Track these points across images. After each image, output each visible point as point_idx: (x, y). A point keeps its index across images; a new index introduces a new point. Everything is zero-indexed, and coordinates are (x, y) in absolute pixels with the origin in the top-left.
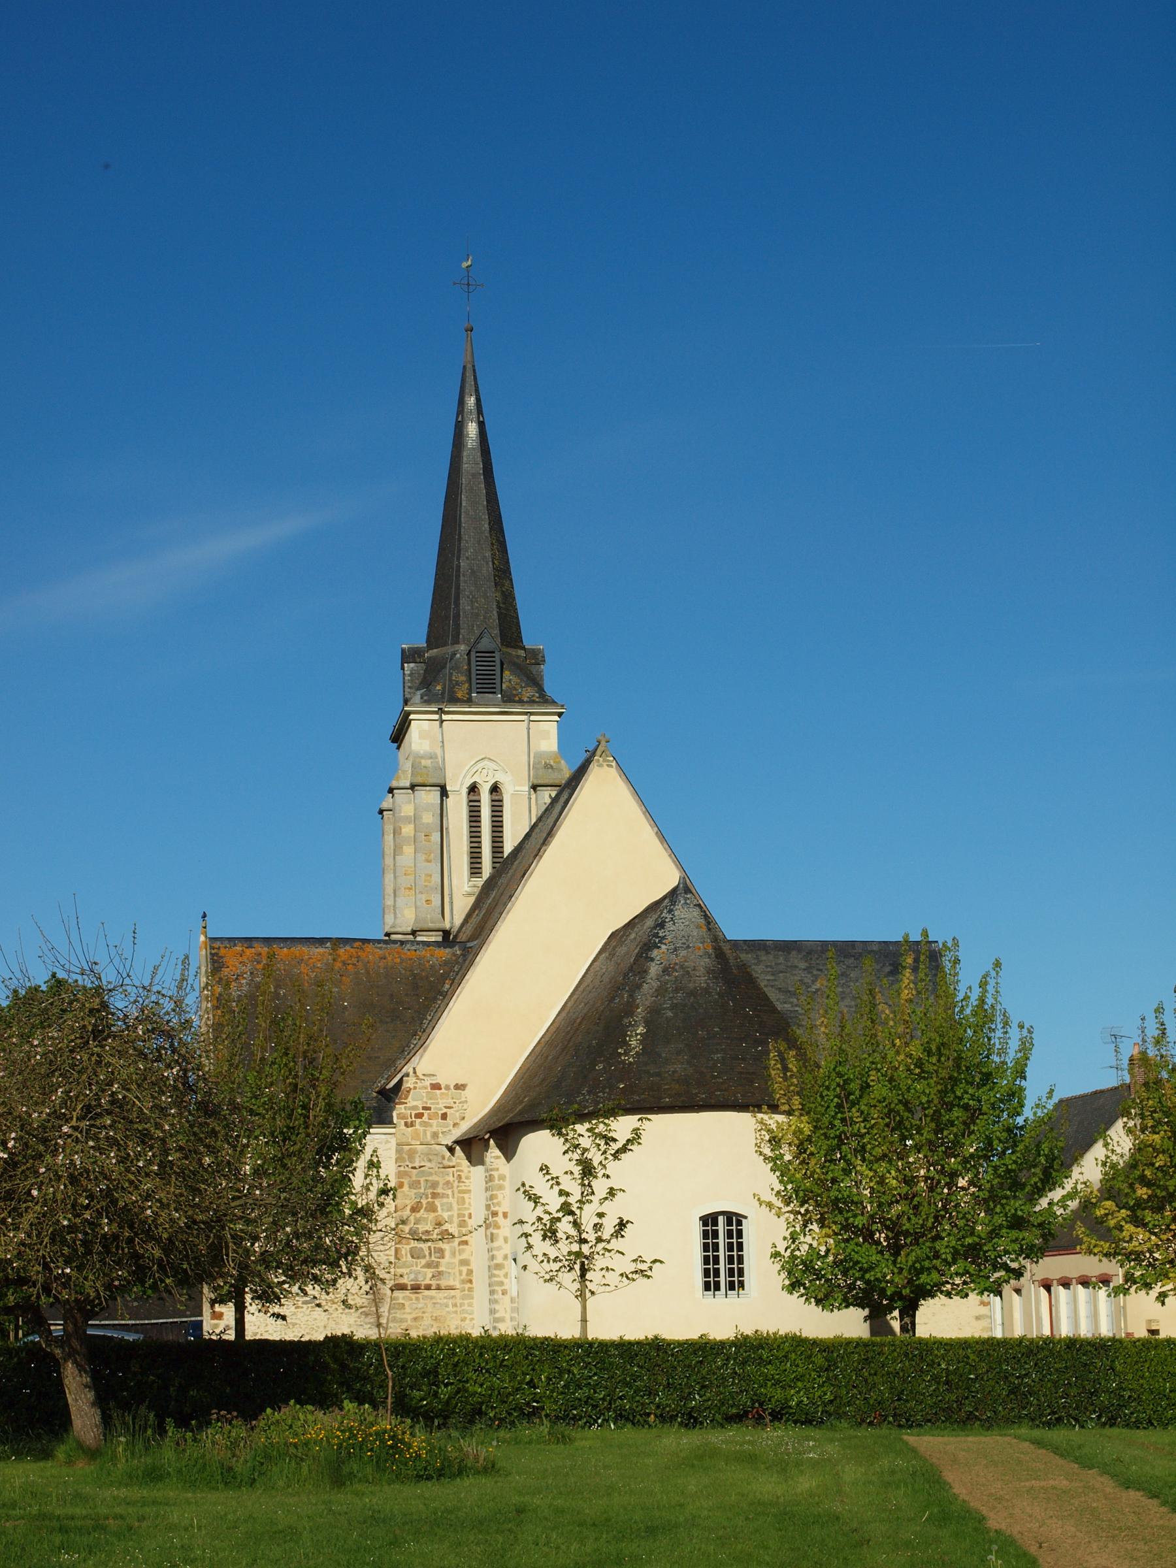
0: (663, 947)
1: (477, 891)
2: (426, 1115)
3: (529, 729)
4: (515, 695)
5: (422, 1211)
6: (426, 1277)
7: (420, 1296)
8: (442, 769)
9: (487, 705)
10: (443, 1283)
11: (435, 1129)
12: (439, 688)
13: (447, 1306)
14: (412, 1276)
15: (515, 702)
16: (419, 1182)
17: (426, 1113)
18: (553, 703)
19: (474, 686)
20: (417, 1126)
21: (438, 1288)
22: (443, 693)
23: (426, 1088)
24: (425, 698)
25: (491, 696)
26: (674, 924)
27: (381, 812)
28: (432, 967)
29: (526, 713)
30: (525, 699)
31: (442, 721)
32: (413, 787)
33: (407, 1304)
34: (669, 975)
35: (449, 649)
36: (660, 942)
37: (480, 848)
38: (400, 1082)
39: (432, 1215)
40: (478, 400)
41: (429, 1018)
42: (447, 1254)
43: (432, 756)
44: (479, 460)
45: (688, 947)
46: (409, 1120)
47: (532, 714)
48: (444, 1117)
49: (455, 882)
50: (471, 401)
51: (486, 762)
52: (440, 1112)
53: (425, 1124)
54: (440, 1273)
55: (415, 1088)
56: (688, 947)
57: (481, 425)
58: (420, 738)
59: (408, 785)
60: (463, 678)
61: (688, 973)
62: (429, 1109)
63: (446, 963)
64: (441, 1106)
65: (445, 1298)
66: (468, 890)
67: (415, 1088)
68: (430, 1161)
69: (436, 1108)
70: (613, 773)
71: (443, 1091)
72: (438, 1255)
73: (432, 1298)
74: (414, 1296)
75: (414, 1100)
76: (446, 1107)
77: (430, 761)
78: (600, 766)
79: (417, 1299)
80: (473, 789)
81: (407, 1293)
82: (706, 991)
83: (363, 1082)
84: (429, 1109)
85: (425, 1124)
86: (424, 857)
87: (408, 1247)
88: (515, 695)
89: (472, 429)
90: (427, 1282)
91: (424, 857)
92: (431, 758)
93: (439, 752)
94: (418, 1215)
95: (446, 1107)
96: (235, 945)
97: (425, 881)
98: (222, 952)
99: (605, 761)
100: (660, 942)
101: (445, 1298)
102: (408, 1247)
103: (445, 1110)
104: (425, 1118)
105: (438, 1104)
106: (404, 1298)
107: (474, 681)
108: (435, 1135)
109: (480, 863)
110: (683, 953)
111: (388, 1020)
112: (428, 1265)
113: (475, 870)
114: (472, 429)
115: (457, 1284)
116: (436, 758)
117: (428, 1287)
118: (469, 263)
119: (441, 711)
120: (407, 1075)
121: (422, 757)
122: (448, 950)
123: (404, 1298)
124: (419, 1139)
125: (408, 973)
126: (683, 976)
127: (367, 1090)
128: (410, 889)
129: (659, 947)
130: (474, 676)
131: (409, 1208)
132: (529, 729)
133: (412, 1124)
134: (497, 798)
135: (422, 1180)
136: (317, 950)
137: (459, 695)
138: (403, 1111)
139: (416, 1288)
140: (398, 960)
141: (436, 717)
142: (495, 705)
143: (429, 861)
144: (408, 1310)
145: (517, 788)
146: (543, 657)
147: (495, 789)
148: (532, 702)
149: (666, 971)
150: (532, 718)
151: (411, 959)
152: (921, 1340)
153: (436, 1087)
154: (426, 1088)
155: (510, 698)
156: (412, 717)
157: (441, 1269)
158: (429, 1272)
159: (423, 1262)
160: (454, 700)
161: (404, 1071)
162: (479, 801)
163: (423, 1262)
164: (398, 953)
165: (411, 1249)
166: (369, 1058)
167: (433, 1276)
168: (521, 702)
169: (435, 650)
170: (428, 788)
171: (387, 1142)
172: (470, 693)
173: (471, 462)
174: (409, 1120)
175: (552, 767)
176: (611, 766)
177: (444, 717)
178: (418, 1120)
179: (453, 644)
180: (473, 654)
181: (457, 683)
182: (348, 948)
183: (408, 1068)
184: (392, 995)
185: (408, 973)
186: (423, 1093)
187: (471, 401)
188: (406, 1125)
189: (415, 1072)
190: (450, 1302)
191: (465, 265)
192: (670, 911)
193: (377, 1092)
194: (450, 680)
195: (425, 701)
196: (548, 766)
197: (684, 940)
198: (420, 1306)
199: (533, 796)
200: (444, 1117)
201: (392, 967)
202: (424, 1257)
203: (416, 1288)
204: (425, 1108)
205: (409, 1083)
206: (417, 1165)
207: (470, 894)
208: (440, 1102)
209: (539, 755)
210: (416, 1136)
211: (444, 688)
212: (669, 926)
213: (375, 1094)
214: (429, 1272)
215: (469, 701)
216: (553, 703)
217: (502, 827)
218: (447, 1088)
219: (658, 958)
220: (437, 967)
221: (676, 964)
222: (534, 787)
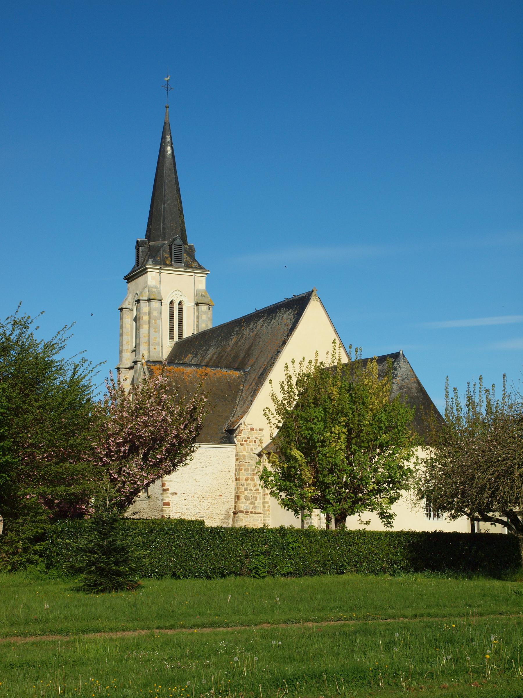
0: (398, 378)
1: (173, 346)
2: (248, 441)
3: (194, 279)
4: (189, 264)
5: (249, 481)
6: (250, 508)
7: (248, 516)
8: (160, 293)
9: (179, 268)
10: (257, 511)
11: (251, 447)
12: (158, 258)
13: (258, 520)
14: (245, 508)
15: (189, 267)
16: (248, 469)
17: (248, 440)
18: (204, 269)
19: (173, 259)
20: (245, 445)
21: (255, 513)
22: (161, 261)
23: (248, 430)
24: (154, 262)
25: (180, 264)
26: (401, 369)
27: (121, 309)
28: (234, 379)
29: (194, 273)
30: (193, 267)
31: (161, 273)
32: (149, 300)
33: (243, 519)
34: (403, 390)
35: (160, 243)
36: (395, 376)
37: (173, 328)
38: (239, 426)
39: (253, 482)
40: (171, 137)
41: (238, 400)
42: (258, 499)
43: (156, 287)
44: (172, 163)
45: (408, 379)
46: (242, 443)
47: (196, 273)
48: (255, 442)
49: (164, 341)
50: (169, 138)
51: (177, 292)
52: (254, 440)
53: (248, 445)
54: (255, 506)
55: (244, 429)
56: (408, 379)
57: (172, 148)
58: (151, 279)
59: (146, 299)
60: (168, 255)
61: (410, 389)
62: (249, 438)
63: (239, 378)
64: (254, 437)
65: (258, 517)
66: (169, 345)
67: (244, 429)
68: (252, 460)
69: (252, 438)
70: (318, 303)
71: (255, 431)
72: (255, 499)
73: (253, 517)
74: (246, 516)
75: (244, 434)
76: (256, 438)
77: (156, 289)
78: (314, 300)
79: (247, 517)
80: (171, 303)
81: (243, 514)
82: (417, 397)
83: (219, 426)
84: (249, 438)
85: (248, 445)
86: (153, 330)
87: (244, 495)
88: (189, 264)
89: (169, 149)
90: (251, 510)
91: (153, 330)
92: (156, 288)
93: (159, 286)
94: (248, 482)
95: (256, 438)
96: (156, 365)
97: (154, 340)
98: (152, 367)
99: (315, 299)
100: (395, 376)
101: (258, 517)
102: (244, 495)
103: (255, 439)
104: (248, 442)
105: (253, 436)
106: (242, 517)
107: (173, 257)
108: (252, 449)
109: (173, 334)
110: (407, 381)
111: (223, 400)
112: (251, 503)
113: (171, 337)
114: (169, 149)
115: (262, 511)
116: (158, 288)
117: (251, 512)
118: (169, 78)
119: (161, 269)
120: (241, 424)
121: (153, 288)
122: (238, 372)
123: (242, 517)
124: (245, 451)
125: (226, 381)
126: (408, 390)
127: (221, 429)
128: (146, 343)
129: (396, 378)
130: (173, 255)
131: (244, 479)
132: (194, 279)
133: (243, 445)
134: (180, 307)
135: (249, 468)
136: (189, 369)
137: (167, 262)
138: (240, 439)
139: (247, 512)
140: (221, 375)
141: (158, 271)
142: (182, 268)
143: (155, 332)
144: (244, 522)
145: (190, 304)
146: (194, 249)
147: (180, 303)
148: (196, 268)
149: (401, 388)
150: (196, 275)
151: (225, 375)
152: (350, 533)
153: (252, 429)
154: (248, 430)
155: (187, 266)
156: (148, 270)
157: (256, 505)
158: (251, 506)
159: (249, 502)
160: (165, 265)
161: (240, 422)
162: (173, 308)
163: (249, 502)
164: (220, 372)
165: (245, 496)
166: (219, 416)
167: (253, 508)
168: (192, 267)
169: (153, 242)
170: (156, 301)
171: (232, 451)
172: (171, 262)
173: (168, 164)
174: (242, 443)
175: (204, 296)
176: (318, 301)
177: (162, 271)
178: (245, 443)
179: (162, 240)
180: (173, 246)
181: (166, 258)
182: (200, 369)
183: (242, 421)
184: (222, 390)
185: (226, 381)
186: (247, 431)
187: (169, 138)
188: (241, 444)
189: (244, 423)
190: (259, 519)
191: (166, 79)
192: (398, 364)
193: (225, 430)
194: (163, 256)
195: (154, 264)
196: (202, 295)
197: (406, 376)
198: (248, 520)
199: (196, 307)
200: (255, 442)
201: (219, 378)
202: (250, 500)
203: (247, 512)
204: (248, 438)
205: (242, 427)
206: (247, 461)
207: (170, 347)
208: (254, 435)
209: (198, 290)
210: (244, 449)
211: (161, 259)
212: (399, 370)
213: (224, 431)
214: (251, 506)
215: (171, 265)
216: (204, 269)
217: (182, 319)
218: (256, 430)
219: (396, 382)
220: (236, 379)
221: (404, 385)
222: (197, 304)
